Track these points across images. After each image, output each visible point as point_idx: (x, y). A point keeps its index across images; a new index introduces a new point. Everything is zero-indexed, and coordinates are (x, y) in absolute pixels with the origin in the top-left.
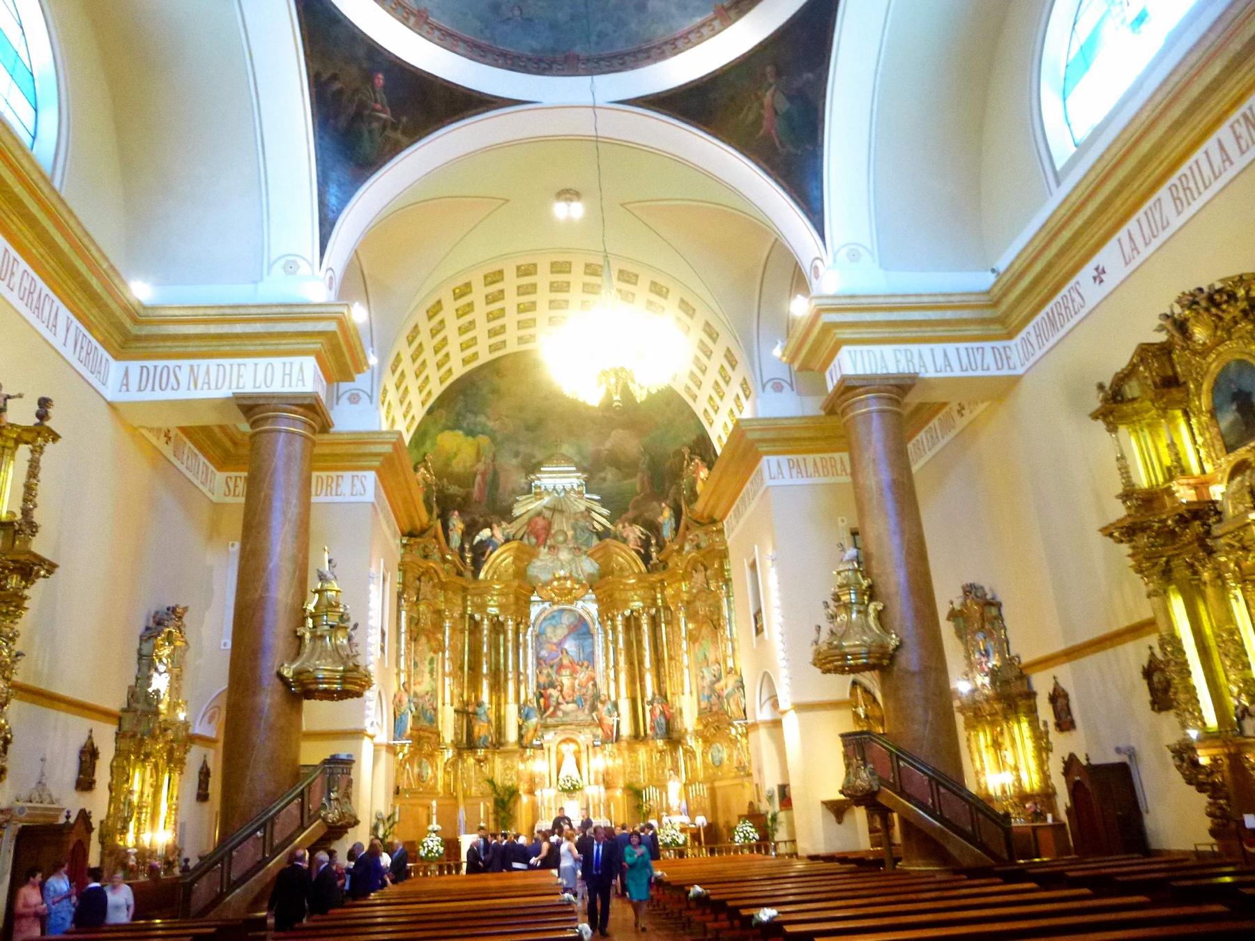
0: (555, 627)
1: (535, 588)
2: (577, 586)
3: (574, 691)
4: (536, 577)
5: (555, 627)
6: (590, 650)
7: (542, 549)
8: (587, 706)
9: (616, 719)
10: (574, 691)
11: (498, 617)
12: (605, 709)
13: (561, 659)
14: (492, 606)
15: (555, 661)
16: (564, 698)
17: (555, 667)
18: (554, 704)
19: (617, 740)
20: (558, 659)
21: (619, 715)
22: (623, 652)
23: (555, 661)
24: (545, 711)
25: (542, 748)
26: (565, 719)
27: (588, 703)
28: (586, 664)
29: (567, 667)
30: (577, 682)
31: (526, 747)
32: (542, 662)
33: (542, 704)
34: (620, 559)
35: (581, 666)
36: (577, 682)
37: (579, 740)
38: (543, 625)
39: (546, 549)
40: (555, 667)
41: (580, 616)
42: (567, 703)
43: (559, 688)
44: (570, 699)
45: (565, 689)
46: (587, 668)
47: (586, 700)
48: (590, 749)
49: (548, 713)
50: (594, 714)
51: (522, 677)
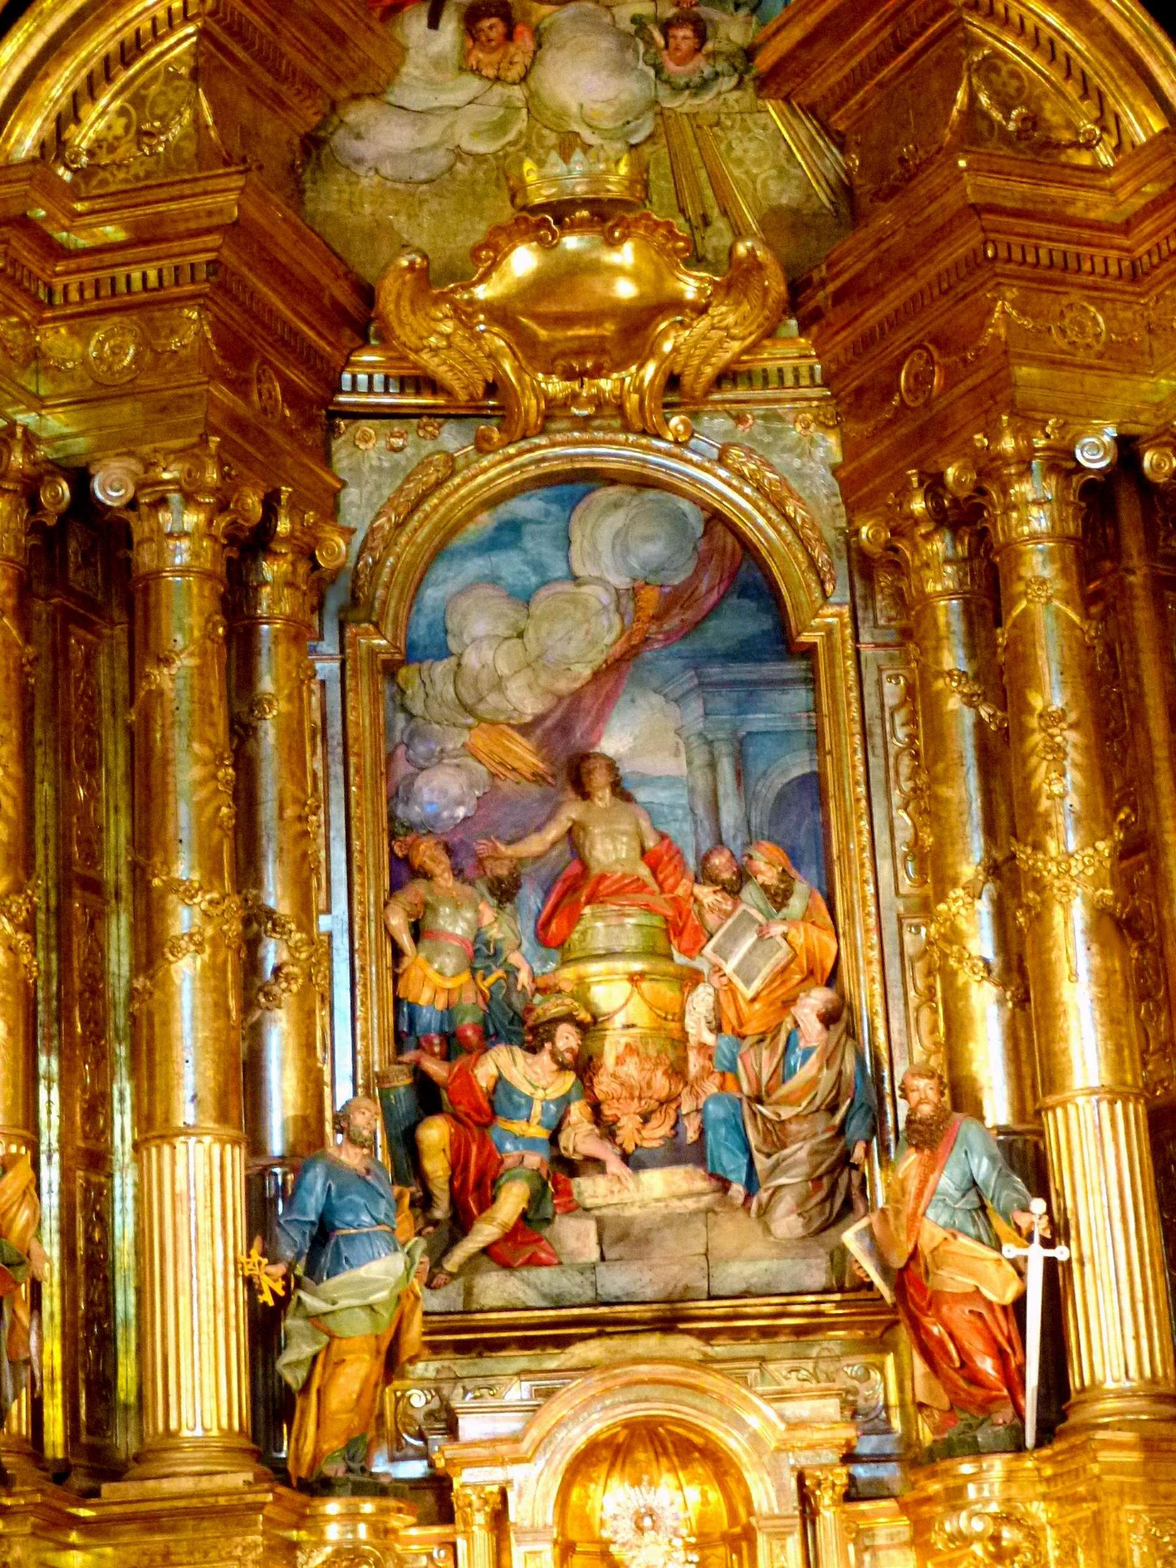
0: (524, 598)
1: (367, 294)
2: (689, 287)
3: (678, 1071)
4: (379, 229)
5: (524, 598)
6: (799, 765)
7: (414, 25)
8: (792, 1178)
9: (1036, 1255)
10: (678, 1071)
11: (80, 478)
12: (947, 1181)
13: (573, 837)
14: (38, 403)
15: (534, 845)
16: (607, 1129)
17: (531, 898)
18: (534, 1160)
19: (1046, 1433)
20: (553, 832)
21: (1059, 1232)
22: (1071, 739)
23: (534, 845)
24: (460, 1224)
25: (445, 1513)
26: (615, 1281)
27: (799, 1151)
28: (768, 875)
29: (628, 888)
30: (701, 1001)
31: (322, 1487)
32: (427, 853)
33: (437, 1166)
34: (1013, 47)
35: (733, 890)
36: (701, 1001)
37: (733, 1442)
38: (432, 595)
39: (450, 25)
40: (531, 898)
41: (715, 518)
42: (633, 1161)
43: (566, 1038)
44: (657, 1133)
45: (612, 1046)
46: (778, 897)
47: (776, 1134)
48: (828, 1514)
49: (485, 1232)
50: (851, 1238)
51: (272, 953)
